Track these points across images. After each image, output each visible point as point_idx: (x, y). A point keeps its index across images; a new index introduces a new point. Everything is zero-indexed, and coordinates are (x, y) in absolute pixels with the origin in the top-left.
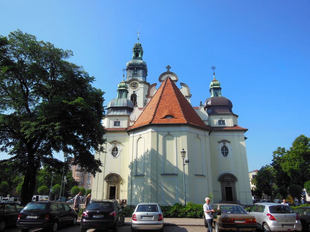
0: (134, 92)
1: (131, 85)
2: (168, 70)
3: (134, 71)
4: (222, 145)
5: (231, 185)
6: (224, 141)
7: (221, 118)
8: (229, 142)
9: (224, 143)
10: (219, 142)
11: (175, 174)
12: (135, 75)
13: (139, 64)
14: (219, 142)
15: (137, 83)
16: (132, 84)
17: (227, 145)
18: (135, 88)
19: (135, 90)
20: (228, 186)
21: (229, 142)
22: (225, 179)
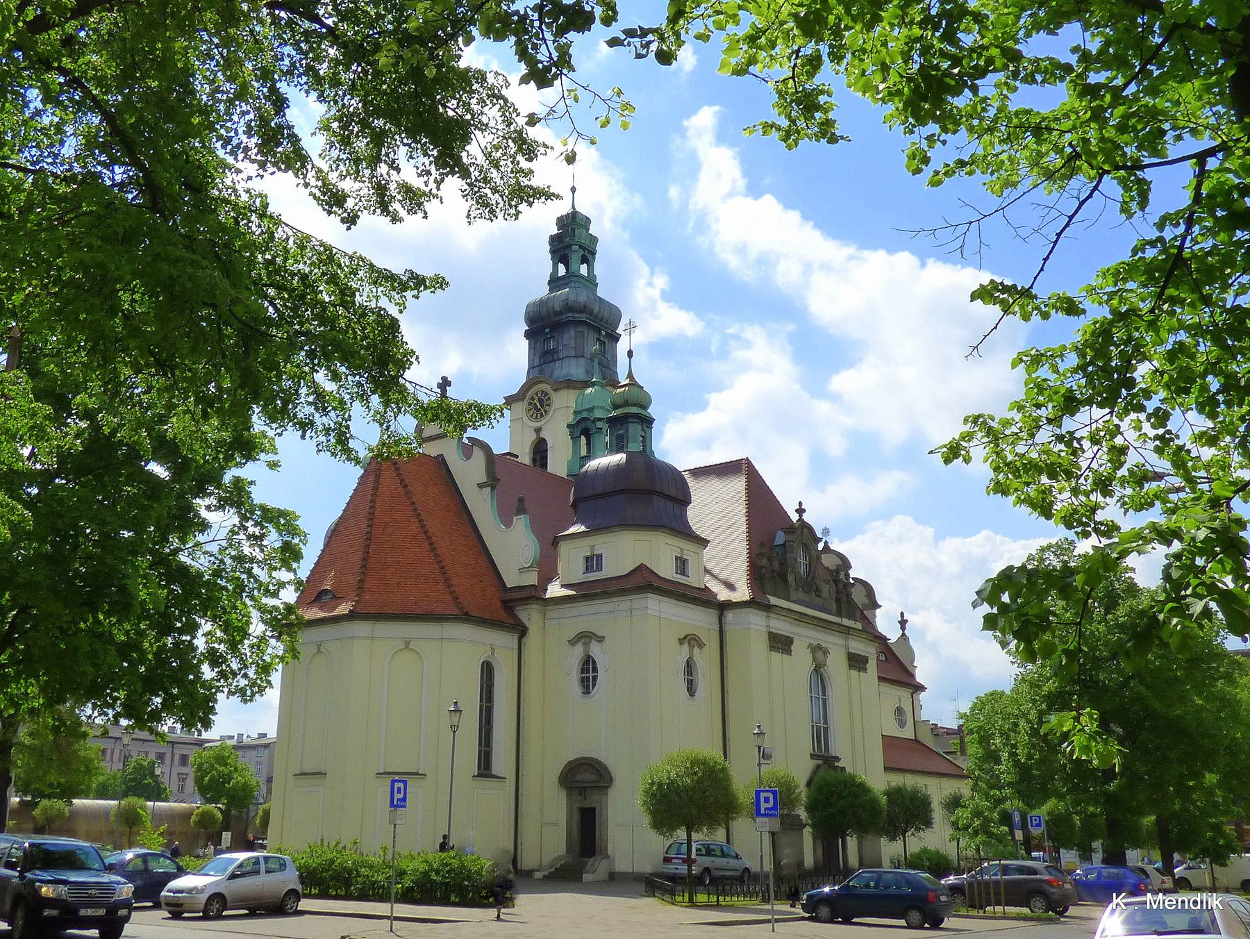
0: (538, 430)
1: (530, 404)
2: (444, 394)
3: (547, 340)
4: (578, 651)
5: (592, 801)
6: (586, 637)
7: (593, 547)
8: (601, 639)
9: (586, 645)
10: (573, 642)
11: (417, 774)
12: (549, 358)
13: (557, 308)
14: (573, 642)
15: (547, 394)
16: (533, 399)
17: (595, 650)
18: (542, 415)
19: (538, 424)
20: (586, 805)
21: (601, 639)
22: (579, 777)
